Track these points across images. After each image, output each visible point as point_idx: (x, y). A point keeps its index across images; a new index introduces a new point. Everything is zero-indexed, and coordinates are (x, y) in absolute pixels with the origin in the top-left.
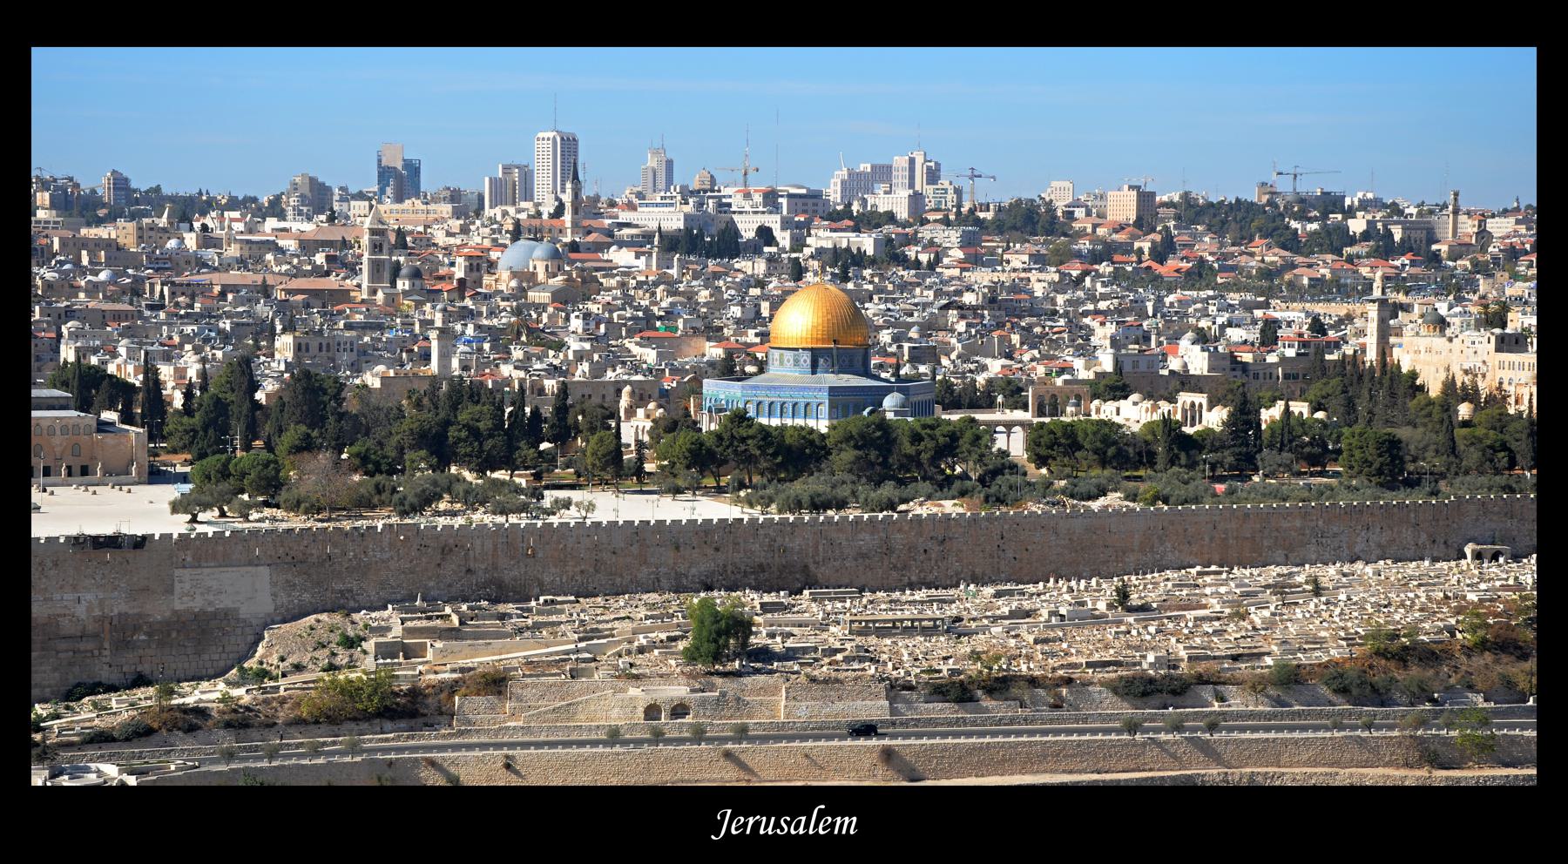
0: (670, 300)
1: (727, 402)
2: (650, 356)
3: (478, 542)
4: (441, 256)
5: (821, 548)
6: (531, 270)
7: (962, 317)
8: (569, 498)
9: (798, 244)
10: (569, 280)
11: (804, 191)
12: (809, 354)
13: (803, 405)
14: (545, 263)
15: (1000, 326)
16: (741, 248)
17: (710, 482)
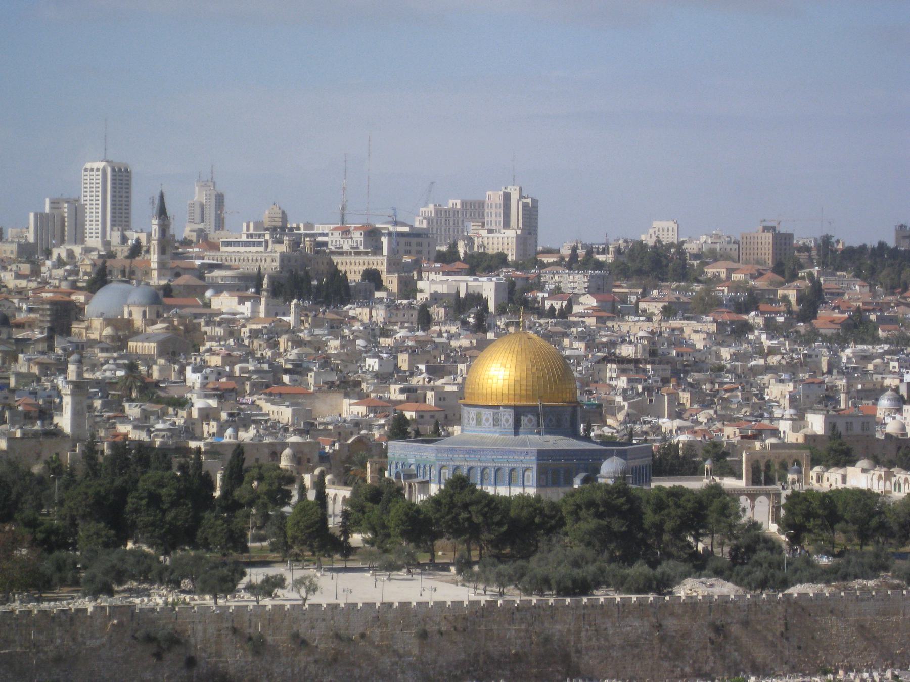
0: (295, 351)
1: (418, 467)
2: (284, 414)
3: (200, 627)
4: (16, 301)
5: (583, 634)
6: (126, 316)
7: (623, 372)
8: (281, 576)
9: (408, 289)
10: (172, 328)
11: (406, 229)
12: (511, 412)
13: (507, 471)
14: (142, 309)
15: (665, 381)
16: (352, 292)
17: (424, 558)
